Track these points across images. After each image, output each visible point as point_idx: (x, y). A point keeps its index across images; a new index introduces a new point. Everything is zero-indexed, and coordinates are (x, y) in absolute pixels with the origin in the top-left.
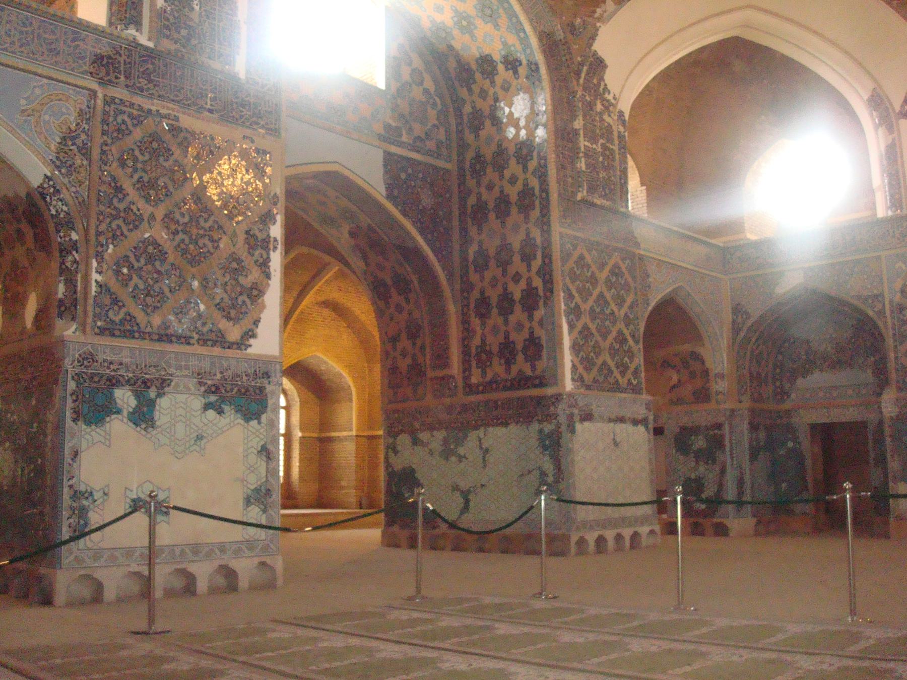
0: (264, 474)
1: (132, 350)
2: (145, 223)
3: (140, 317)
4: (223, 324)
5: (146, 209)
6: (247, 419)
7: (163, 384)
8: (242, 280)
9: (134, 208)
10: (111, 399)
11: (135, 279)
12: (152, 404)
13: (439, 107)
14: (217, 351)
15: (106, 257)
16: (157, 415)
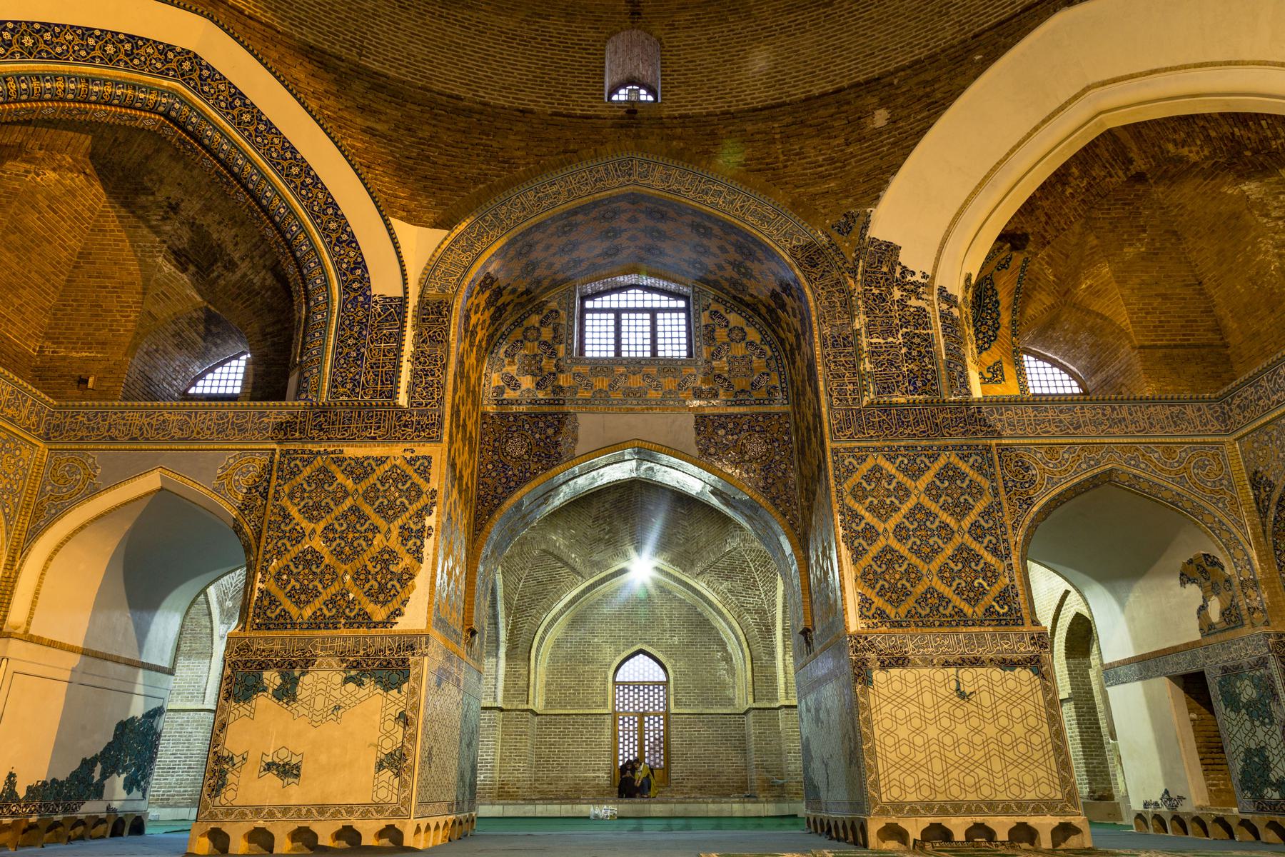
0: (400, 739)
1: (283, 638)
2: (307, 538)
3: (294, 611)
4: (370, 608)
5: (307, 525)
6: (387, 688)
7: (307, 664)
8: (393, 568)
9: (298, 528)
10: (259, 679)
11: (293, 582)
12: (295, 681)
13: (769, 353)
14: (362, 631)
15: (270, 569)
16: (299, 690)
